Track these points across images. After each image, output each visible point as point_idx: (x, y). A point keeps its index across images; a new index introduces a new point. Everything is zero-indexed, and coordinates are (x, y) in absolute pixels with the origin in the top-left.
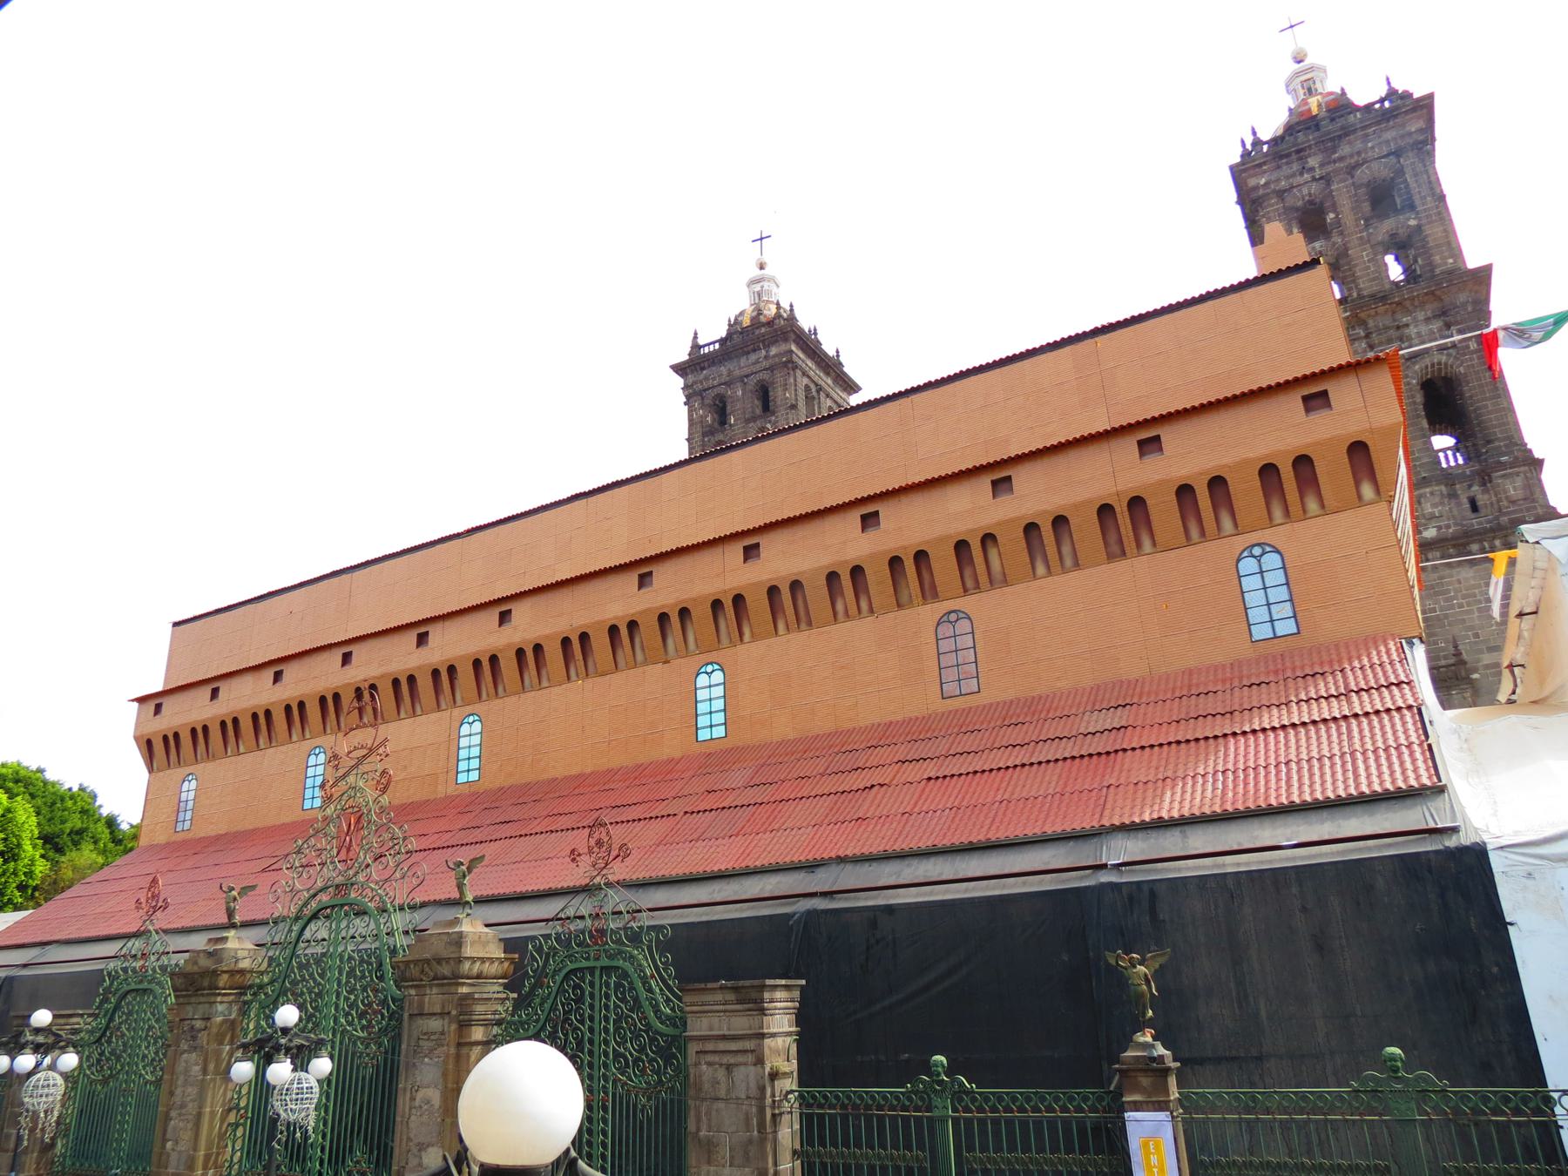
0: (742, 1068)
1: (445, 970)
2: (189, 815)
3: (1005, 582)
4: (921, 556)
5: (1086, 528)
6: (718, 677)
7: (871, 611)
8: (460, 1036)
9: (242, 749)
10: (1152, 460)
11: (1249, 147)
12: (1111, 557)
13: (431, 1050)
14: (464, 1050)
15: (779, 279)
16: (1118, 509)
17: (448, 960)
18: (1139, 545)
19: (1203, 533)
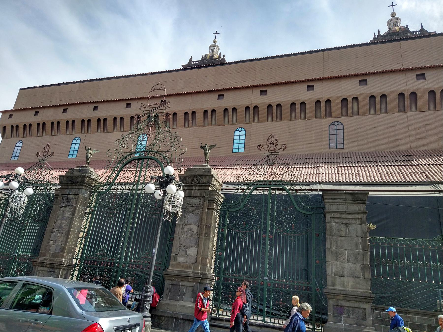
0: (354, 225)
1: (205, 180)
2: (17, 155)
3: (358, 114)
4: (328, 101)
5: (393, 101)
6: (243, 132)
7: (305, 118)
8: (209, 206)
9: (44, 134)
10: (421, 81)
11: (376, 36)
12: (400, 111)
13: (193, 211)
14: (210, 211)
15: (220, 47)
16: (406, 95)
17: (206, 176)
18: (411, 109)
19: (435, 108)
